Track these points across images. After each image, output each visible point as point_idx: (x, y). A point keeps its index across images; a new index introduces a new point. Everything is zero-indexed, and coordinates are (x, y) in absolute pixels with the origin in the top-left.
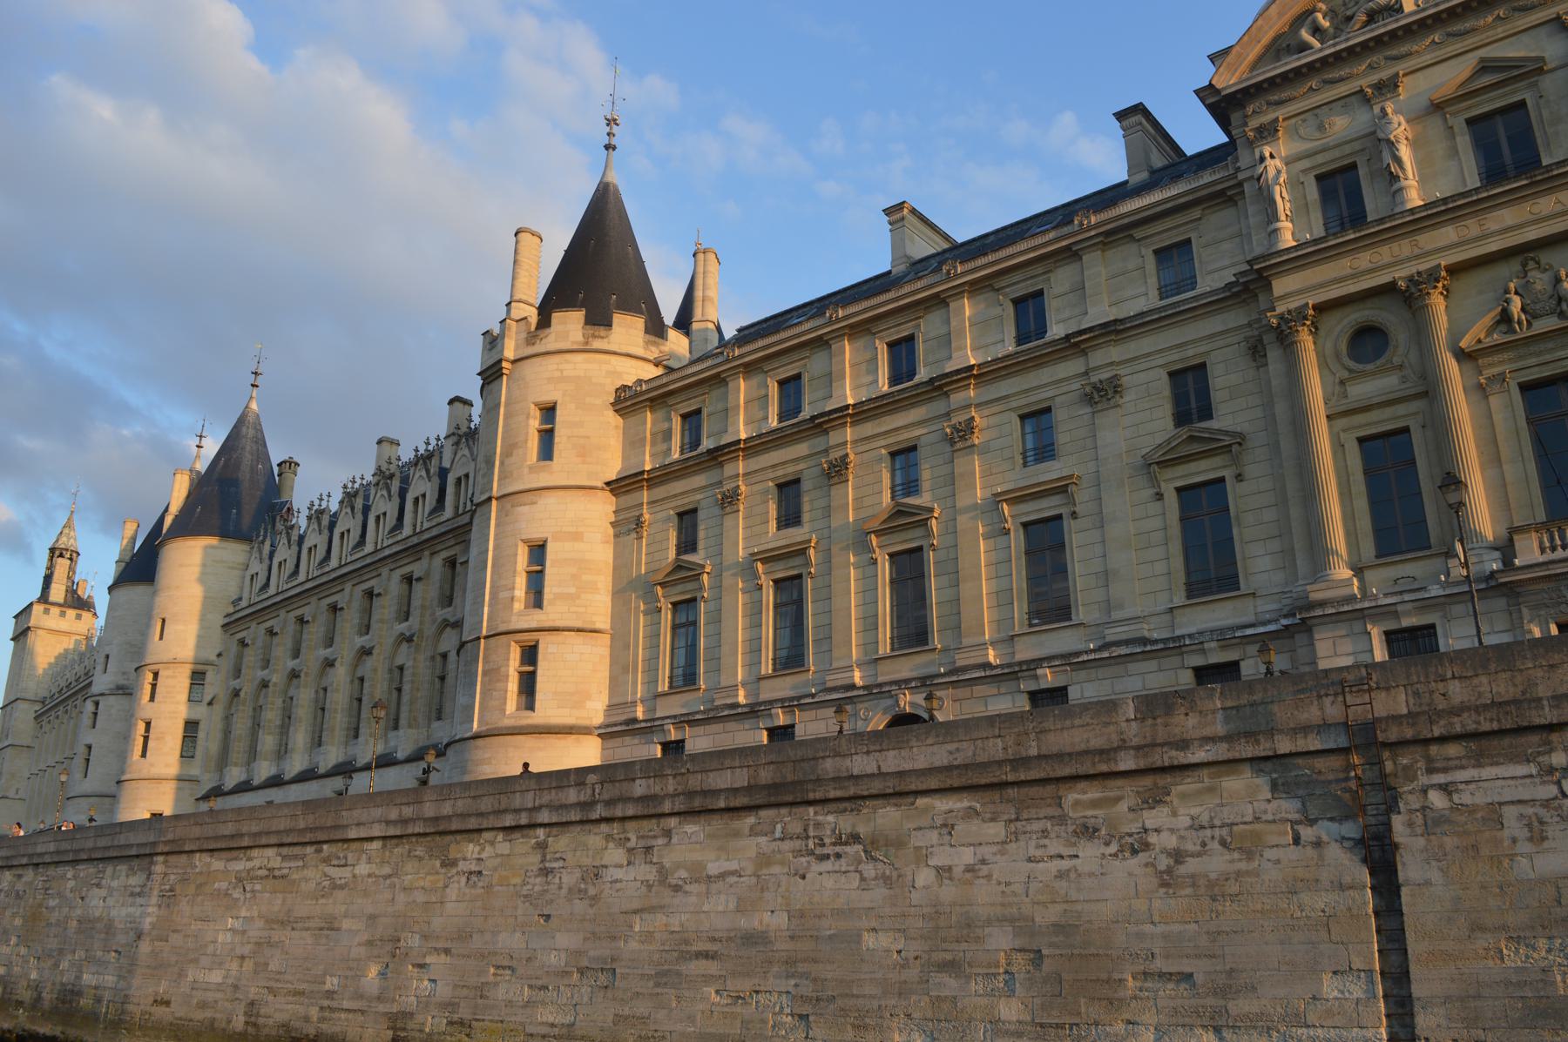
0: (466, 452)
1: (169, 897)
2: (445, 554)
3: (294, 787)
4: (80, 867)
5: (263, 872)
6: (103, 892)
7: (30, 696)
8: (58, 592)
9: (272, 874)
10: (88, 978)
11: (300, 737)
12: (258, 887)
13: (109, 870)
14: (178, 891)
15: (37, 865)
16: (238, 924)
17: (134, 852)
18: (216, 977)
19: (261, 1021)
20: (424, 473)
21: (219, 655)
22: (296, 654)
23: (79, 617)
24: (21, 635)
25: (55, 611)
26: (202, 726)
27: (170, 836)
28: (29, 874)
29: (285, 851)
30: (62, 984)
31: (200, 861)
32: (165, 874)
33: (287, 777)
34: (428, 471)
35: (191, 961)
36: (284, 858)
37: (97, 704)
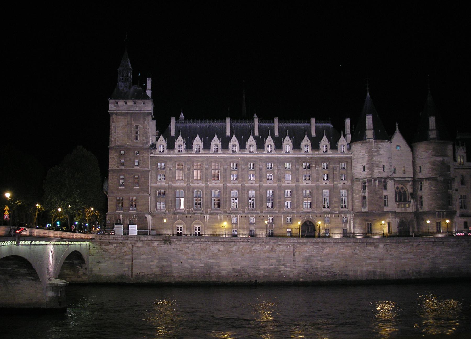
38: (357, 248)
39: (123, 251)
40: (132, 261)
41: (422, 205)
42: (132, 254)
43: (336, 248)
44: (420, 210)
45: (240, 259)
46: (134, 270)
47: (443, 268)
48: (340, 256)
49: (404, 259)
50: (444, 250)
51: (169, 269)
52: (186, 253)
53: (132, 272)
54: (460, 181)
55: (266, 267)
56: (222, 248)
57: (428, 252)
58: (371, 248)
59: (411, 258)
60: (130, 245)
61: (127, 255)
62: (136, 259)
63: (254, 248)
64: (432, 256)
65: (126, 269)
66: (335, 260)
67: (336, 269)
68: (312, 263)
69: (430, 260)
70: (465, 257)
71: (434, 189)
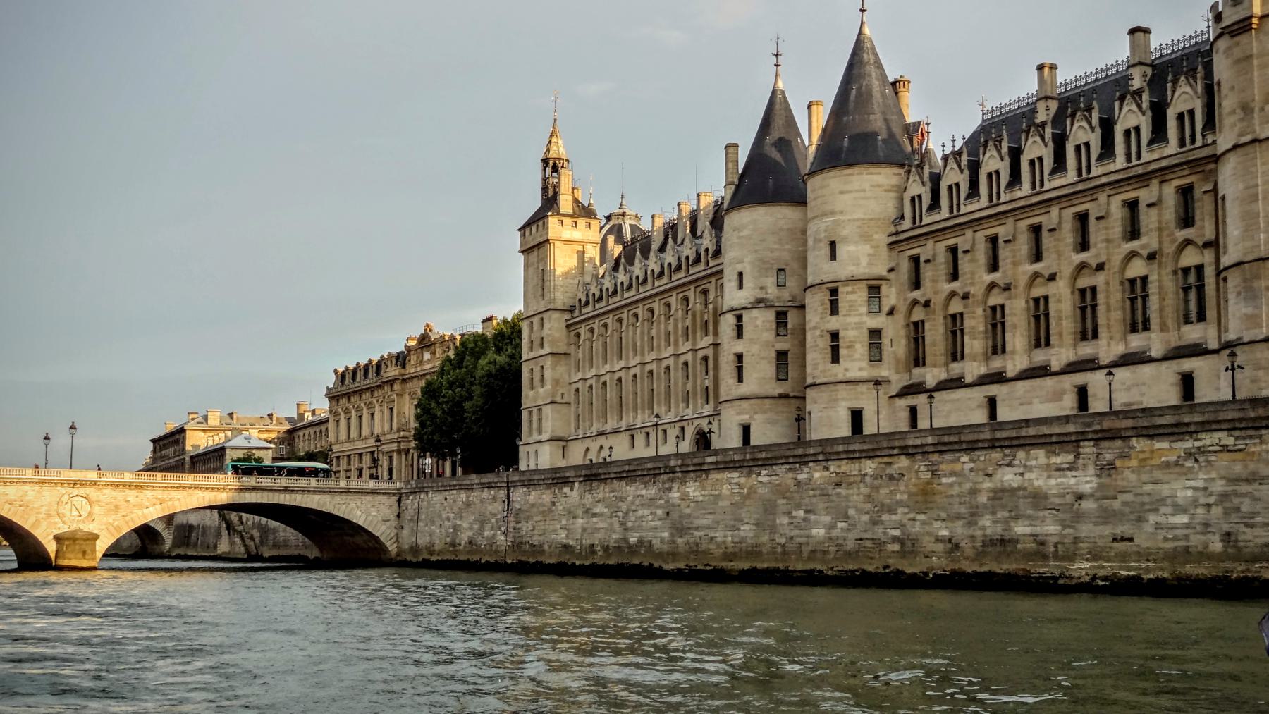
0: (1188, 89)
1: (1107, 469)
2: (1177, 183)
3: (1020, 384)
4: (977, 453)
5: (1217, 448)
6: (1017, 470)
7: (559, 305)
8: (566, 204)
9: (1225, 449)
10: (1021, 529)
11: (1017, 339)
12: (1213, 458)
13: (1021, 454)
14: (1118, 463)
15: (913, 454)
16: (1200, 484)
17: (1054, 439)
18: (1183, 519)
19: (1241, 544)
20: (1134, 107)
21: (891, 270)
22: (994, 266)
23: (589, 225)
24: (535, 246)
25: (567, 221)
26: (884, 334)
27: (1097, 427)
28: (903, 462)
29: (1237, 433)
30: (985, 536)
31: (1139, 444)
32: (1098, 454)
33: (1010, 374)
34: (1139, 106)
35: (1150, 510)
36: (1237, 438)
37: (739, 318)
58: (566, 490)
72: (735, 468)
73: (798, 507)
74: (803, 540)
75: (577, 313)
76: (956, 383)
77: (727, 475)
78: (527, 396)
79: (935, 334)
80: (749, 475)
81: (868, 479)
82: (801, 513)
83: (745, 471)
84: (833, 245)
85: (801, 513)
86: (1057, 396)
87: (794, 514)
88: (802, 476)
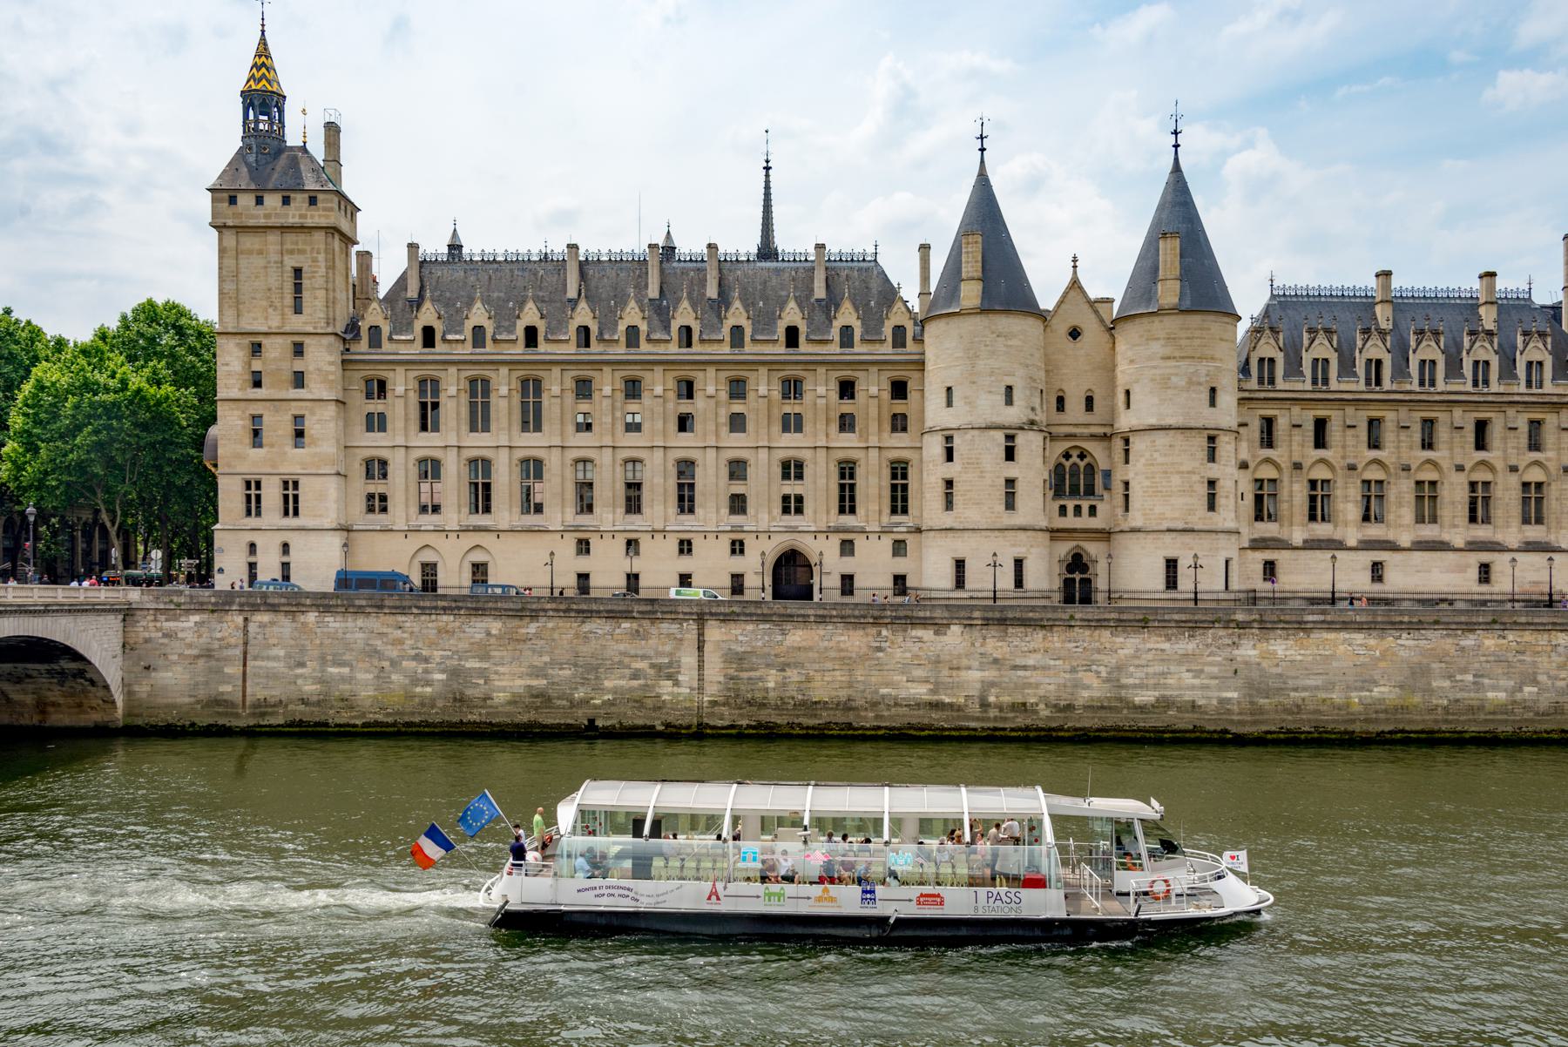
38: (884, 632)
39: (219, 635)
40: (245, 665)
41: (1127, 509)
42: (246, 644)
43: (822, 633)
44: (1125, 527)
45: (546, 659)
46: (249, 690)
47: (1145, 697)
48: (833, 654)
49: (1025, 668)
50: (1149, 646)
51: (347, 687)
52: (401, 642)
53: (244, 696)
54: (1257, 435)
55: (622, 683)
56: (495, 626)
57: (1099, 651)
58: (927, 634)
59: (1045, 668)
60: (240, 620)
61: (229, 646)
62: (255, 659)
63: (587, 627)
64: (1112, 660)
65: (228, 688)
66: (817, 666)
67: (819, 693)
68: (753, 674)
69: (1104, 674)
70: (1215, 670)
71: (1160, 460)
72: (1360, 629)
73: (1464, 671)
74: (1474, 703)
75: (363, 345)
76: (1339, 545)
77: (1343, 635)
78: (240, 457)
79: (1295, 495)
80: (1383, 638)
81: (1560, 649)
82: (1470, 678)
83: (1375, 633)
84: (1213, 390)
85: (1470, 678)
86: (1462, 569)
87: (1459, 677)
88: (1469, 641)
